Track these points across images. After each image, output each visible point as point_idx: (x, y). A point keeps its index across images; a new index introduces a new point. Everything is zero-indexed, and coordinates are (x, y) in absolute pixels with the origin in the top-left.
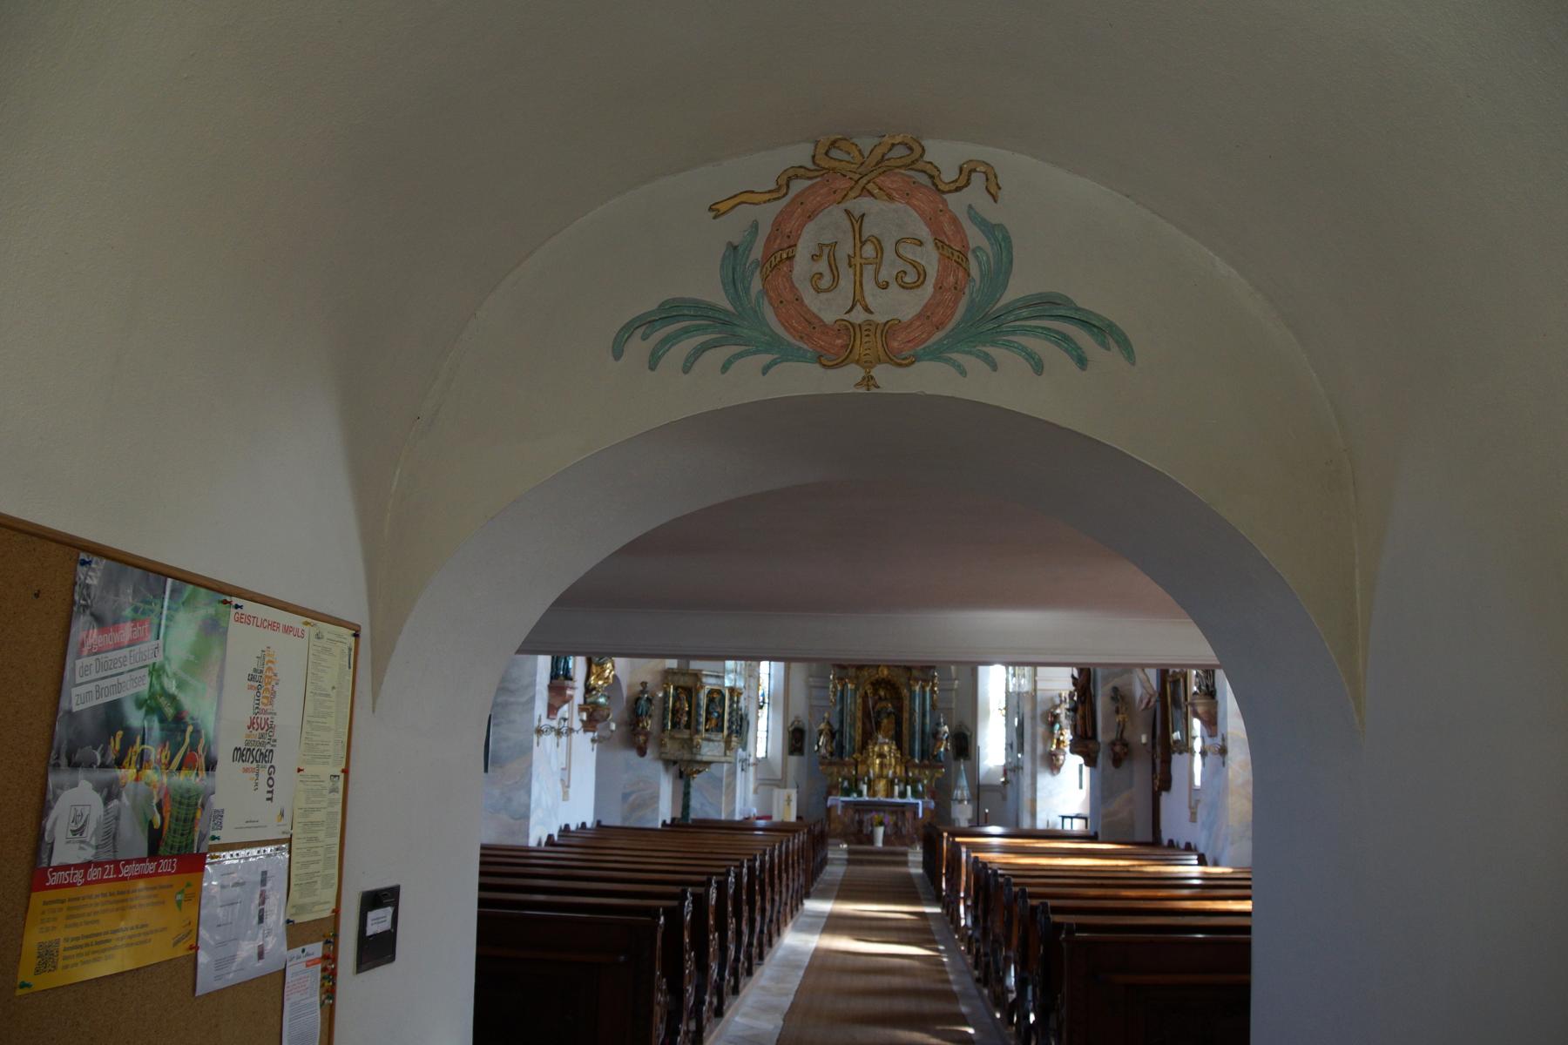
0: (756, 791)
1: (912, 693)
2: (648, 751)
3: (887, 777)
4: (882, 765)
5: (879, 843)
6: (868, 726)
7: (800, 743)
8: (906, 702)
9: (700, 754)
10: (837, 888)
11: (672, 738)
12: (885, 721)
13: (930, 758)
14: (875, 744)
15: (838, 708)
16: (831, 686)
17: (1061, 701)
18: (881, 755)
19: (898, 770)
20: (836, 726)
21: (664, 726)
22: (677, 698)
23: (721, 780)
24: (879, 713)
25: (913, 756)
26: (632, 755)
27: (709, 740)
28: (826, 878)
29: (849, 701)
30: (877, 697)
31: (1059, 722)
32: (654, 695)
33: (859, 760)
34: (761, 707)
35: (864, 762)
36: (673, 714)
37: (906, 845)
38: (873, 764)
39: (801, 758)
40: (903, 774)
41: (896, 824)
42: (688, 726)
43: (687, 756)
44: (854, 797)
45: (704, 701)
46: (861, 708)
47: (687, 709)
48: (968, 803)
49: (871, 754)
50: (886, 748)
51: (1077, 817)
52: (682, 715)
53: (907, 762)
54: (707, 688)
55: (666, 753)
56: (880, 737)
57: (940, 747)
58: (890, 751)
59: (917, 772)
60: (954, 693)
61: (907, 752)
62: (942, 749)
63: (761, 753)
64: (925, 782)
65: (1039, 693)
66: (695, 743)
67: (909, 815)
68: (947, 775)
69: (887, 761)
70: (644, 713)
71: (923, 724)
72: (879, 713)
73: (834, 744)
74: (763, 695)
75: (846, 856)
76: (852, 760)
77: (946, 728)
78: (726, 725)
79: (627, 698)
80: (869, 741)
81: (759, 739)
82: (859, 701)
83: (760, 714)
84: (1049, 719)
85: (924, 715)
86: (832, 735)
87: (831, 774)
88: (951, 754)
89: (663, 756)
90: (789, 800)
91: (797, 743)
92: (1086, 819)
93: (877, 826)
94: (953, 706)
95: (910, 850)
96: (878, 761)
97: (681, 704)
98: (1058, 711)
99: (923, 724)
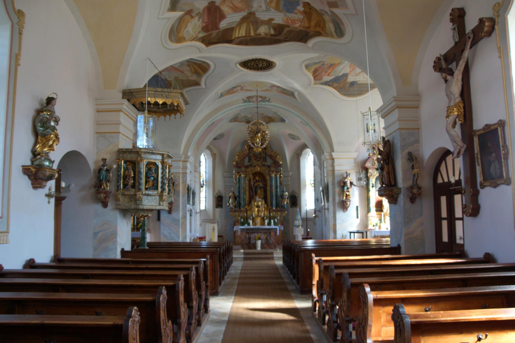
0: (201, 225)
1: (271, 178)
2: (109, 204)
3: (261, 216)
4: (258, 211)
5: (259, 248)
6: (251, 194)
8: (269, 182)
9: (142, 205)
10: (237, 281)
11: (123, 195)
12: (259, 191)
13: (280, 207)
14: (255, 201)
15: (238, 186)
16: (234, 176)
17: (347, 175)
18: (258, 207)
19: (266, 213)
20: (237, 194)
21: (118, 186)
22: (126, 169)
23: (179, 221)
24: (256, 187)
26: (99, 207)
27: (148, 195)
28: (232, 272)
29: (242, 182)
30: (255, 181)
31: (347, 186)
32: (111, 168)
33: (248, 209)
34: (202, 187)
35: (250, 210)
36: (124, 179)
37: (271, 248)
38: (254, 210)
39: (222, 209)
40: (268, 215)
41: (267, 238)
42: (133, 186)
43: (133, 206)
44: (246, 226)
45: (143, 170)
46: (248, 185)
47: (133, 175)
48: (302, 227)
49: (253, 206)
50: (260, 203)
51: (357, 232)
52: (129, 179)
53: (270, 209)
54: (145, 162)
55: (120, 205)
56: (257, 198)
57: (284, 202)
58: (262, 205)
59: (274, 213)
60: (289, 177)
61: (269, 204)
62: (285, 203)
63: (203, 207)
64: (279, 218)
65: (336, 172)
66: (137, 197)
67: (272, 234)
68: (288, 214)
69: (260, 209)
70: (104, 179)
71: (276, 192)
72: (256, 187)
73: (236, 202)
74: (203, 181)
75: (243, 256)
77: (287, 193)
78: (160, 185)
79: (94, 170)
80: (252, 200)
81: (201, 202)
82: (247, 182)
83: (201, 190)
84: (342, 184)
86: (235, 198)
87: (235, 216)
88: (289, 205)
89: (118, 207)
90: (214, 229)
91: (219, 202)
92: (362, 233)
93: (257, 240)
94: (290, 183)
95: (274, 252)
96: (256, 209)
97: (128, 172)
98: (346, 180)
99: (276, 192)
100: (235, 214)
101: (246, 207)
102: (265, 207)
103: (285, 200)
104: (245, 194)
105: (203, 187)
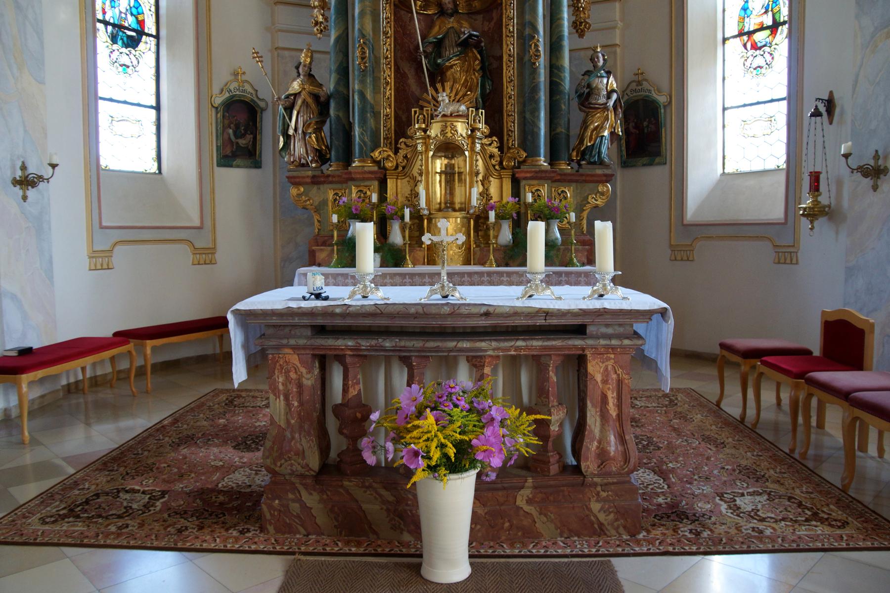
3: (464, 208)
4: (450, 175)
6: (412, 81)
7: (249, 137)
15: (333, 35)
18: (449, 148)
19: (493, 190)
20: (330, 85)
24: (439, 44)
25: (533, 152)
33: (389, 165)
35: (404, 170)
38: (425, 173)
40: (508, 197)
46: (391, 32)
49: (419, 148)
50: (461, 128)
53: (514, 167)
56: (443, 97)
57: (600, 128)
58: (472, 137)
59: (544, 191)
61: (514, 140)
69: (462, 164)
71: (554, 69)
72: (439, 44)
76: (370, 166)
77: (613, 83)
85: (555, 47)
96: (439, 164)
99: (554, 69)
100: (316, 195)
102: (492, 156)
103: (607, 119)
104: (376, 80)
105: (142, 46)
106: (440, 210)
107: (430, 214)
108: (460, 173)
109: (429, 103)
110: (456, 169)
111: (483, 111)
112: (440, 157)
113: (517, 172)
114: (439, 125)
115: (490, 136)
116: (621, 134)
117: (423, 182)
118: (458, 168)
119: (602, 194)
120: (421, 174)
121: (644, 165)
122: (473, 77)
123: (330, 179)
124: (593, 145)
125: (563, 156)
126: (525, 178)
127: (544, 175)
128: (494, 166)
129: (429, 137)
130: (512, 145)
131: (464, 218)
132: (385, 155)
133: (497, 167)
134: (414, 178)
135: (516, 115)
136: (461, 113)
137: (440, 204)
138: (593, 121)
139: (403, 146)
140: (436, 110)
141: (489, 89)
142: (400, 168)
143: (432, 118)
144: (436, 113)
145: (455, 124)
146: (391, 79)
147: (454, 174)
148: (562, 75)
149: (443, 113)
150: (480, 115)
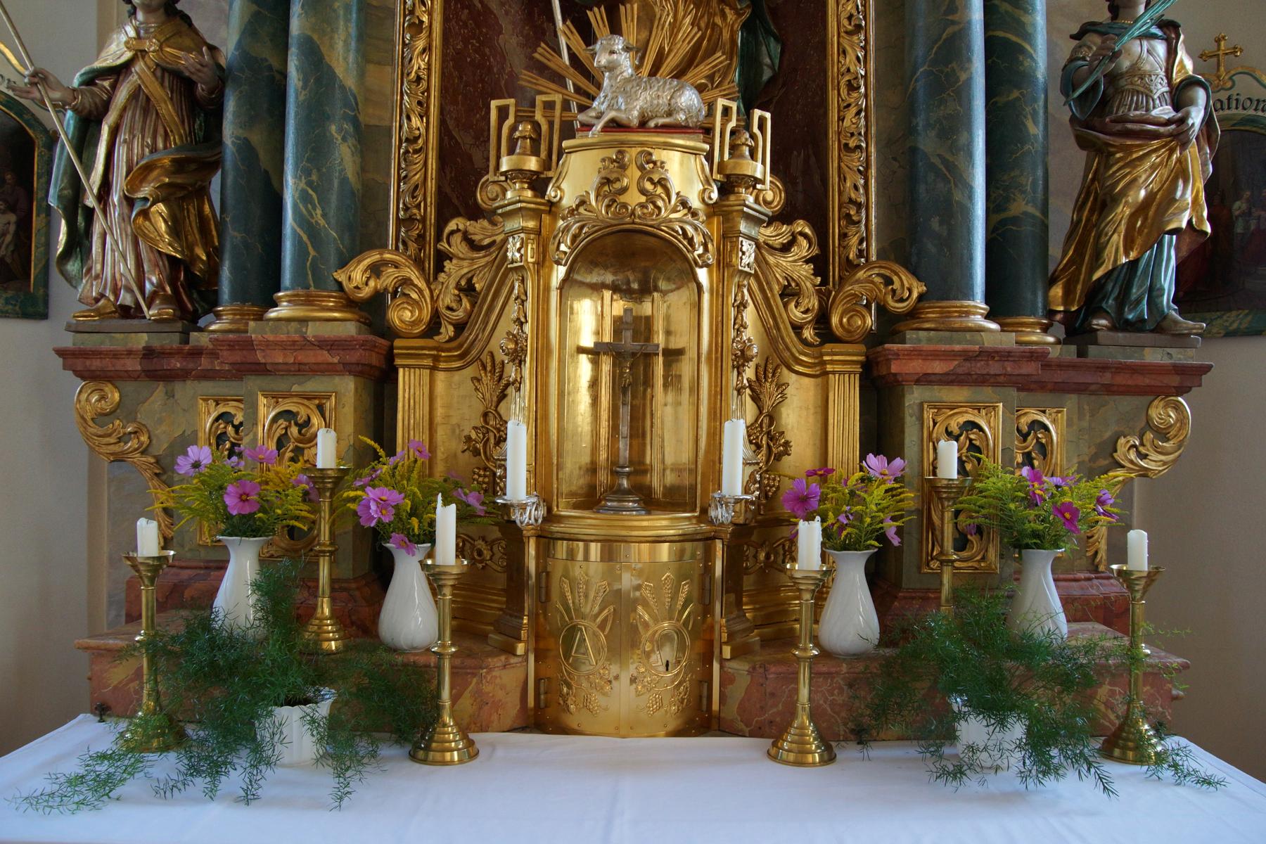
33: (401, 316)
101: (356, 276)
102: (790, 292)
106: (590, 500)
107: (550, 517)
108: (673, 355)
109: (559, 79)
110: (660, 339)
111: (768, 115)
112: (597, 288)
113: (897, 355)
114: (595, 156)
115: (784, 216)
116: (1209, 229)
117: (527, 386)
118: (668, 333)
119: (1163, 434)
120: (518, 357)
121: (1231, 334)
122: (718, 21)
123: (205, 363)
124: (1134, 264)
125: (1029, 296)
126: (925, 380)
127: (995, 368)
128: (797, 328)
129: (552, 206)
130: (860, 254)
131: (685, 538)
132: (389, 278)
133: (808, 333)
134: (497, 371)
135: (873, 149)
136: (681, 117)
137: (593, 469)
138: (1134, 180)
139: (457, 246)
140: (583, 108)
141: (772, 67)
142: (448, 331)
143: (568, 131)
144: (582, 117)
145: (658, 155)
146: (430, 14)
147: (648, 357)
148: (1025, 19)
149: (612, 114)
150: (756, 130)
